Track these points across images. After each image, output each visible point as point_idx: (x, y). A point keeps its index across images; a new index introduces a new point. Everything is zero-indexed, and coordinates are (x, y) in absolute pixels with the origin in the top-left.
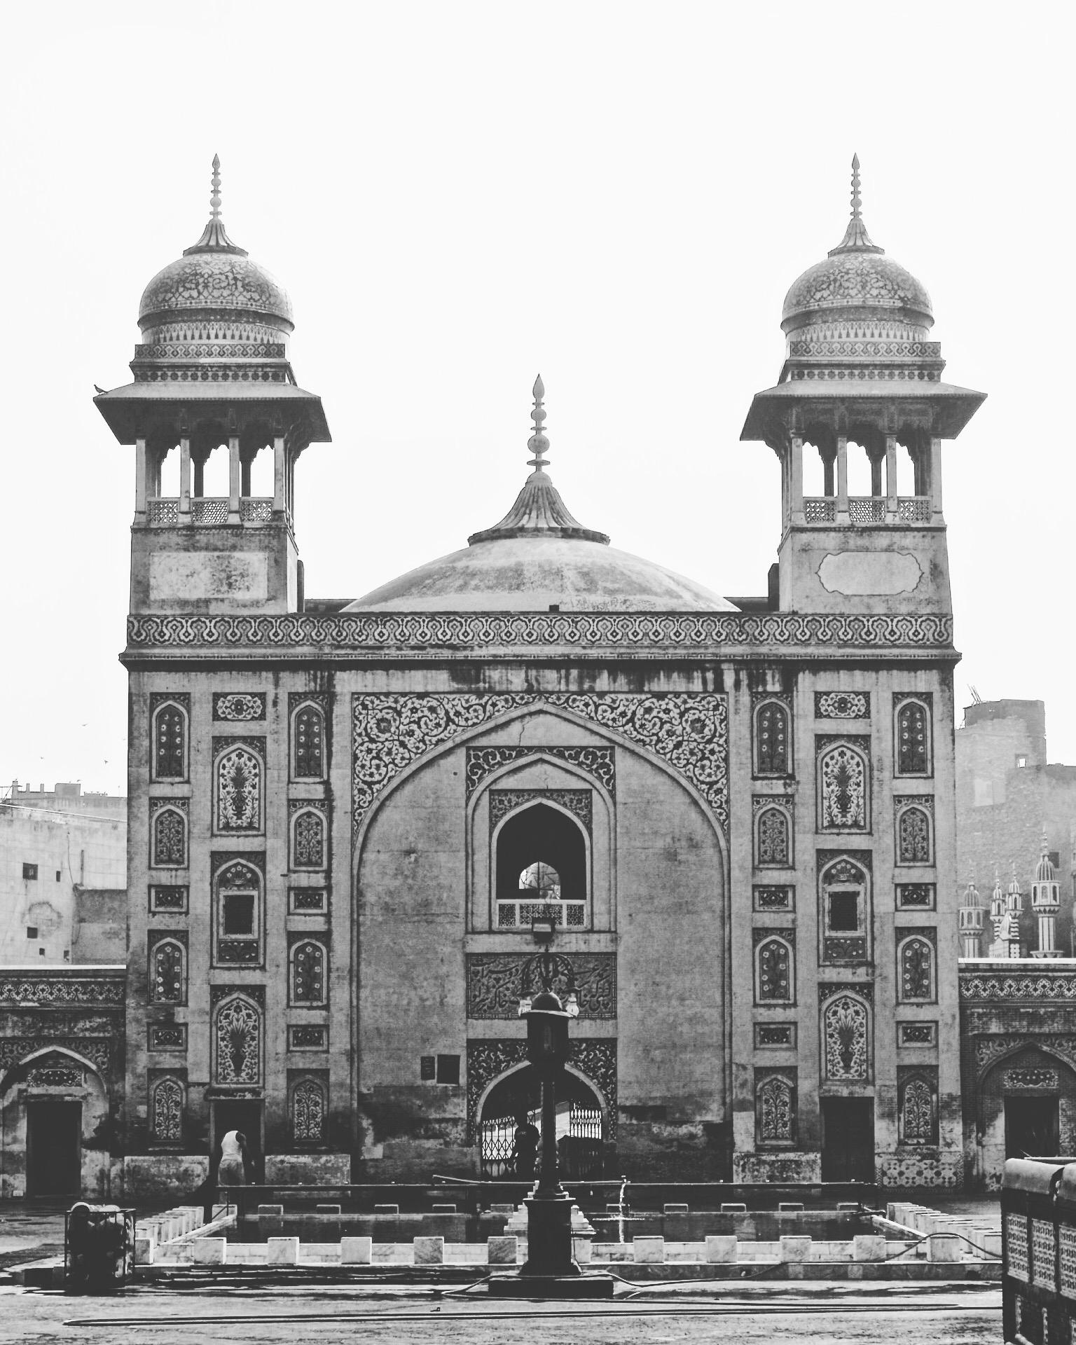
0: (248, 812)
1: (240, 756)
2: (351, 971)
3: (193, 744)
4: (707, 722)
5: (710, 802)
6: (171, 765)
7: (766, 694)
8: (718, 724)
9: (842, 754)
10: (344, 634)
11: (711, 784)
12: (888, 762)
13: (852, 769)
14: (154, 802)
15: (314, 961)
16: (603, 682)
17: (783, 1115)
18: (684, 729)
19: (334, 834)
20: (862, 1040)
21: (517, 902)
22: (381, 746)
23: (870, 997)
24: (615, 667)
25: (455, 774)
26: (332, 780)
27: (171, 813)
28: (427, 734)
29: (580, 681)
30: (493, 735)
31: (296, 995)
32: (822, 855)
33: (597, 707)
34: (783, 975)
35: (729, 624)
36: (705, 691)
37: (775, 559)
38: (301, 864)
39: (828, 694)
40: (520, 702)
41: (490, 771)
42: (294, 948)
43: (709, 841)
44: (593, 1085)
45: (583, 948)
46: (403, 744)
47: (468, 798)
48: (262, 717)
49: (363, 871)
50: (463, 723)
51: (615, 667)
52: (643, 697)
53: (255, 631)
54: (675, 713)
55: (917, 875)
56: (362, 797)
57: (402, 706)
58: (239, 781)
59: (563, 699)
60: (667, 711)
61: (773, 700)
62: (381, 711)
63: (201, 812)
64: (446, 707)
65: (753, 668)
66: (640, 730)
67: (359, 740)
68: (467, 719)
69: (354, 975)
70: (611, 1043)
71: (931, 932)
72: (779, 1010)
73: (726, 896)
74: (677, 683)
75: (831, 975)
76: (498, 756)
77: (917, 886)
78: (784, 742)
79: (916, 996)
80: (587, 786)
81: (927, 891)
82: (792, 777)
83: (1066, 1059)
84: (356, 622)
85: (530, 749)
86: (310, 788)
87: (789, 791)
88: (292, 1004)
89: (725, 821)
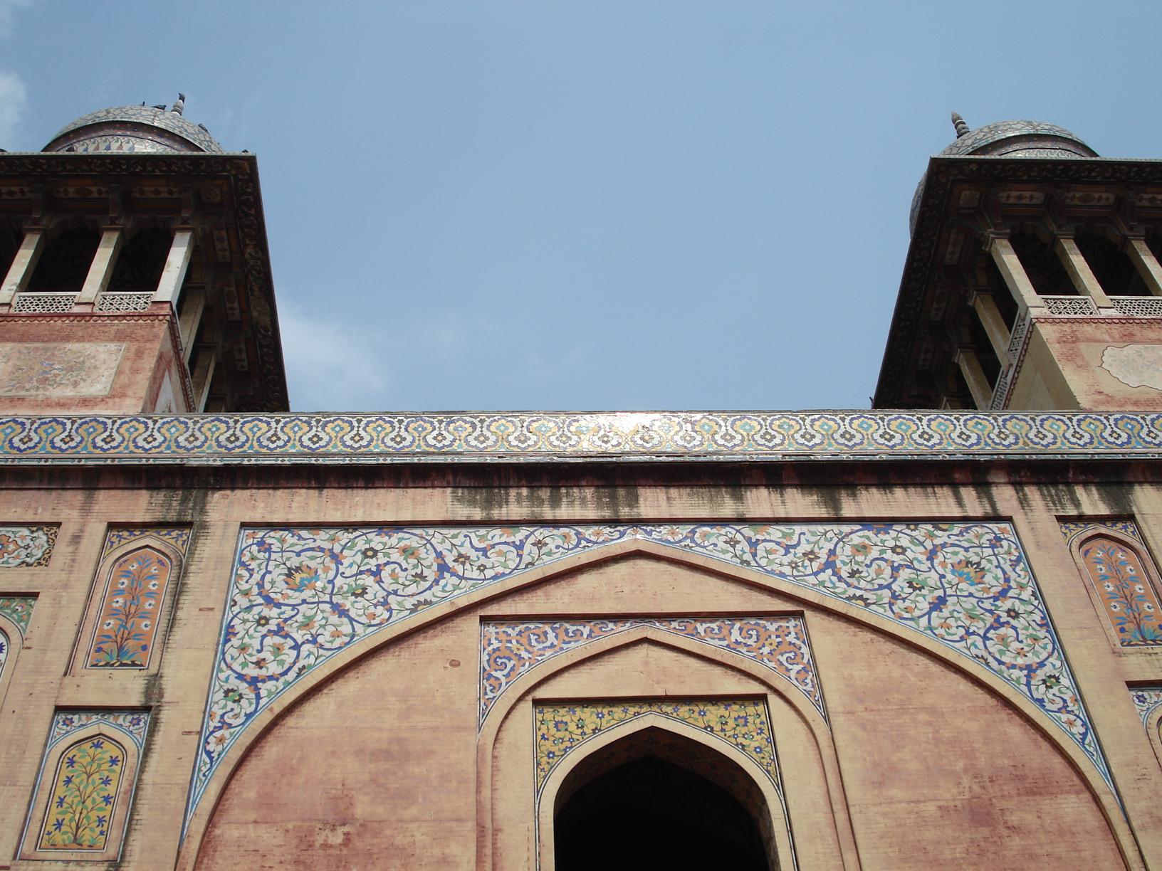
4: (984, 564)
5: (1041, 702)
8: (1008, 569)
10: (243, 438)
11: (1030, 670)
16: (760, 501)
18: (942, 576)
19: (147, 777)
22: (289, 612)
25: (455, 664)
26: (165, 671)
28: (395, 593)
33: (754, 544)
35: (977, 423)
38: (54, 846)
40: (593, 538)
46: (341, 611)
48: (44, 561)
50: (476, 574)
52: (846, 529)
53: (69, 436)
54: (916, 553)
56: (230, 705)
57: (344, 547)
61: (1102, 530)
62: (298, 554)
64: (439, 548)
66: (849, 580)
67: (243, 602)
68: (482, 568)
74: (904, 501)
76: (551, 635)
80: (757, 689)
84: (268, 423)
89: (1084, 735)
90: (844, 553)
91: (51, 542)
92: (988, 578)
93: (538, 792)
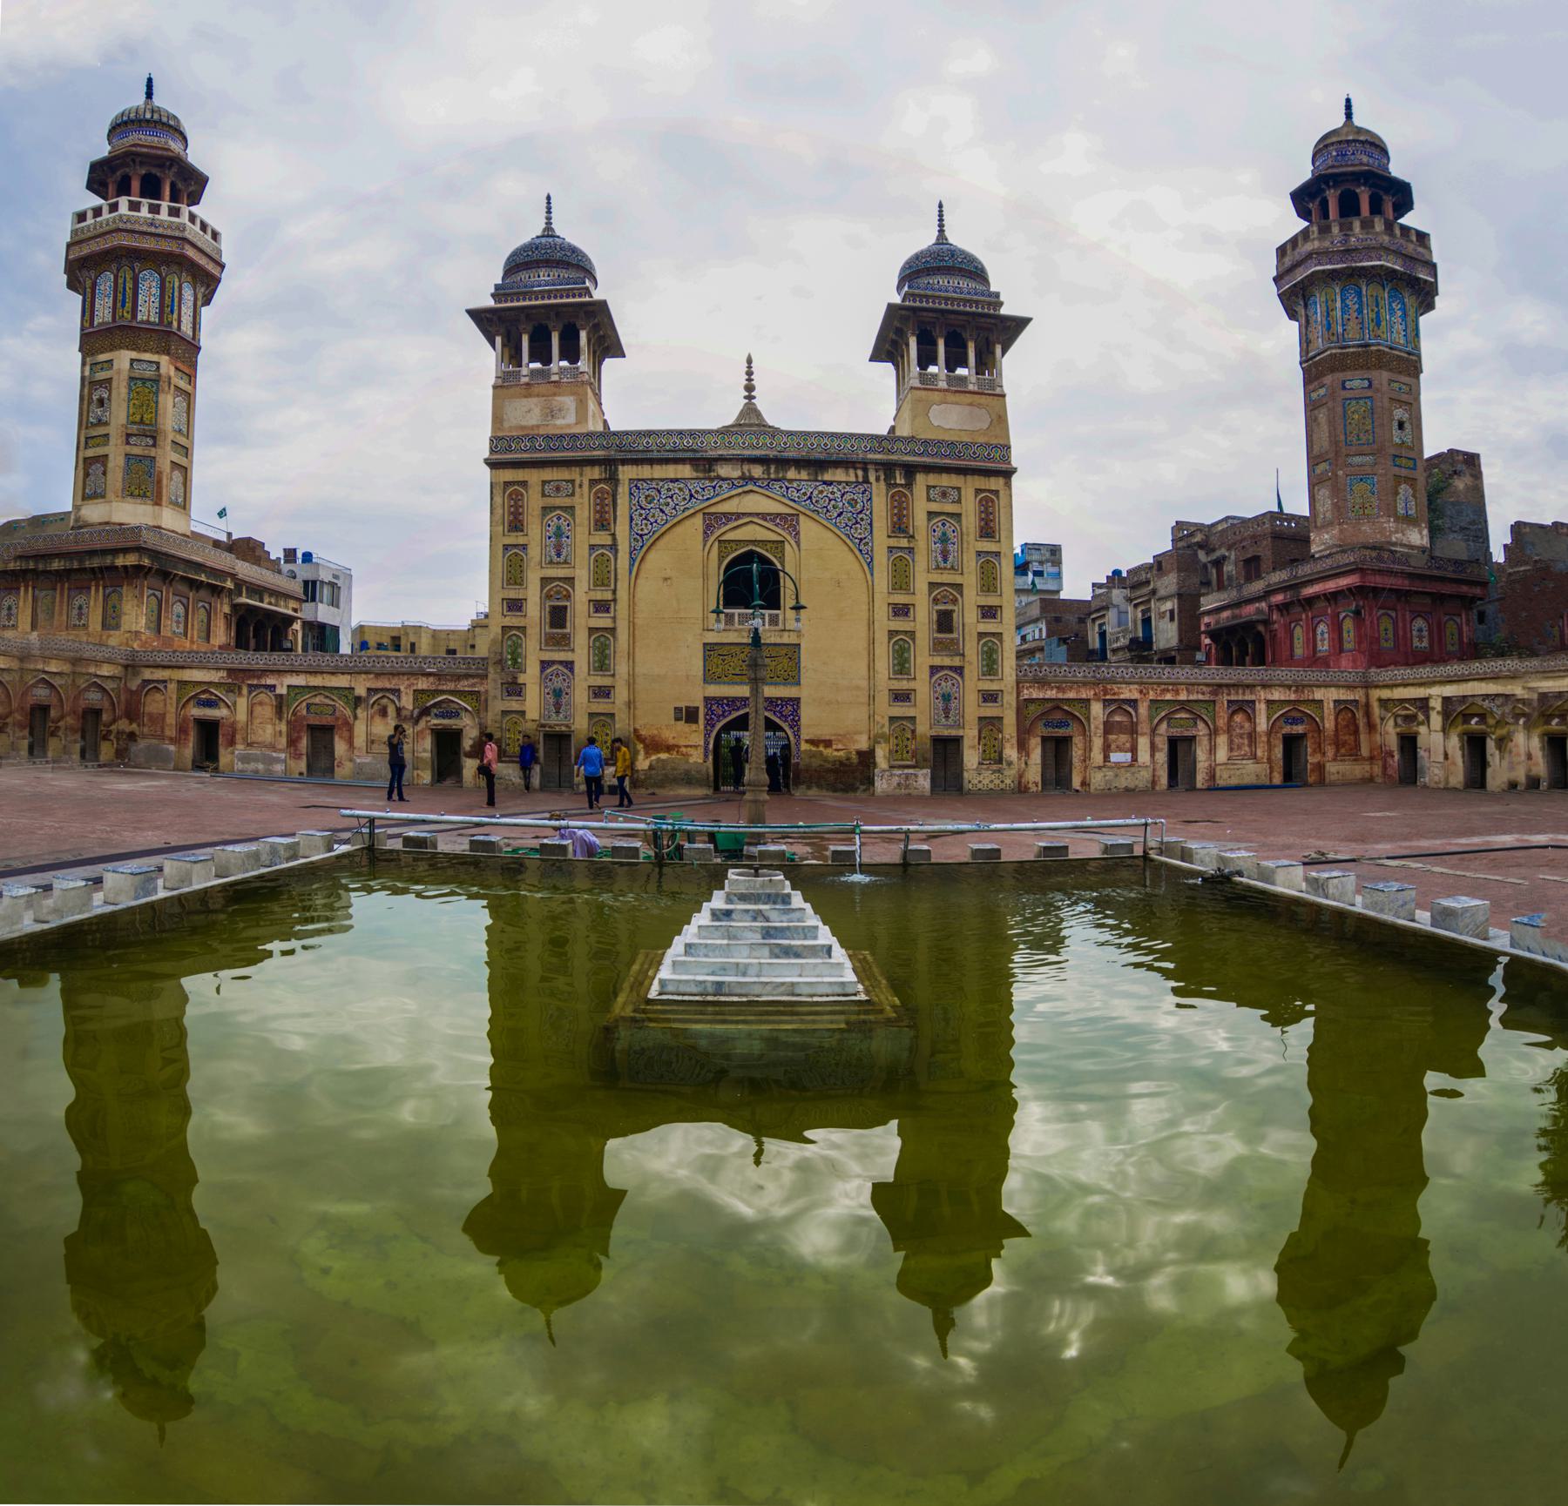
0: (564, 554)
1: (559, 519)
2: (629, 653)
3: (530, 511)
5: (861, 551)
6: (516, 525)
7: (896, 485)
9: (944, 525)
11: (861, 539)
12: (972, 530)
13: (950, 534)
14: (506, 547)
15: (608, 647)
17: (906, 746)
20: (956, 701)
21: (736, 611)
23: (961, 674)
24: (799, 463)
26: (617, 533)
27: (516, 554)
29: (777, 472)
30: (720, 505)
31: (594, 668)
32: (933, 585)
33: (788, 488)
34: (907, 660)
36: (857, 482)
37: (893, 423)
38: (598, 586)
39: (934, 487)
41: (719, 528)
42: (592, 638)
43: (861, 575)
44: (785, 726)
45: (778, 641)
46: (663, 512)
47: (705, 545)
48: (573, 494)
49: (638, 589)
51: (799, 463)
54: (838, 495)
55: (991, 601)
58: (559, 533)
59: (766, 483)
60: (833, 493)
63: (534, 552)
65: (888, 468)
69: (631, 656)
70: (798, 700)
71: (999, 635)
72: (905, 682)
73: (871, 609)
74: (839, 475)
75: (938, 661)
77: (991, 607)
78: (908, 515)
79: (990, 675)
80: (780, 539)
81: (996, 611)
82: (913, 537)
83: (1077, 714)
85: (744, 514)
86: (603, 538)
87: (911, 545)
88: (592, 673)
90: (816, 492)
91: (573, 486)
92: (858, 506)
93: (719, 568)
